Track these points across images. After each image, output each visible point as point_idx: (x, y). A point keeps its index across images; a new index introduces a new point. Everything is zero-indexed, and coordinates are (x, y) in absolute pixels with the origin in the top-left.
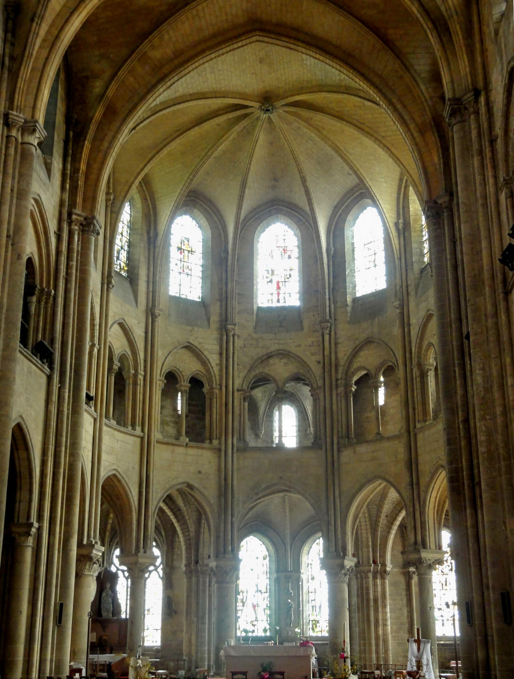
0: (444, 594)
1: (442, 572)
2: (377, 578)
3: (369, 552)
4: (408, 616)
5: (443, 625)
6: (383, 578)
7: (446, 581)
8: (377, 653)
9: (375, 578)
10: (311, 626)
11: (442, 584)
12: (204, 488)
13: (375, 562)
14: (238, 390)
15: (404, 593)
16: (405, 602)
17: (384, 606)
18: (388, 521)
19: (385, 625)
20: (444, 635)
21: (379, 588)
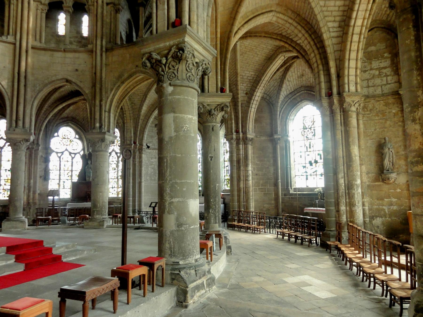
0: (308, 155)
1: (307, 137)
2: (240, 144)
3: (232, 123)
4: (274, 173)
5: (307, 179)
6: (245, 144)
7: (310, 145)
8: (239, 201)
9: (238, 144)
10: (226, 183)
11: (307, 147)
12: (81, 82)
13: (237, 132)
14: (107, 4)
15: (271, 155)
16: (272, 161)
17: (246, 165)
18: (248, 98)
19: (246, 180)
20: (307, 186)
21: (242, 152)
